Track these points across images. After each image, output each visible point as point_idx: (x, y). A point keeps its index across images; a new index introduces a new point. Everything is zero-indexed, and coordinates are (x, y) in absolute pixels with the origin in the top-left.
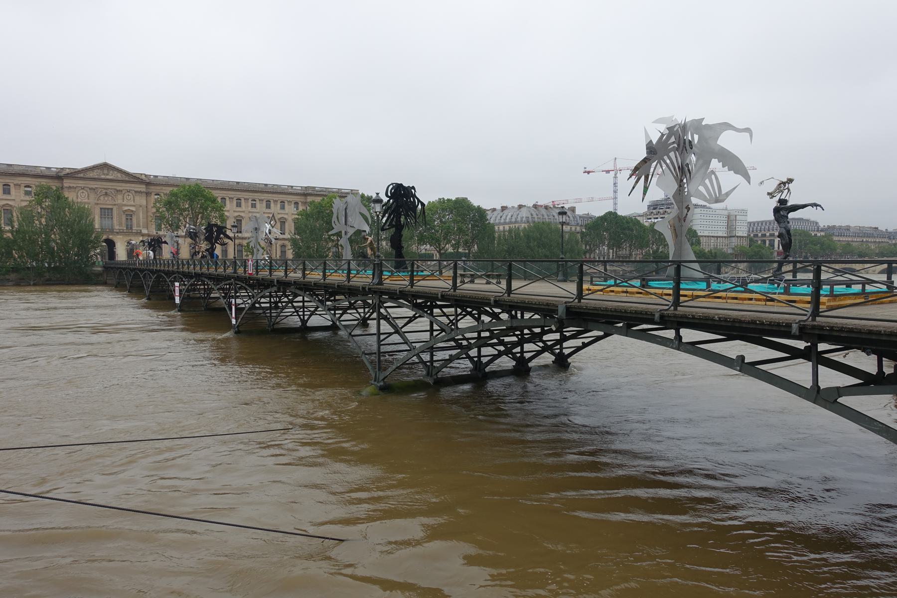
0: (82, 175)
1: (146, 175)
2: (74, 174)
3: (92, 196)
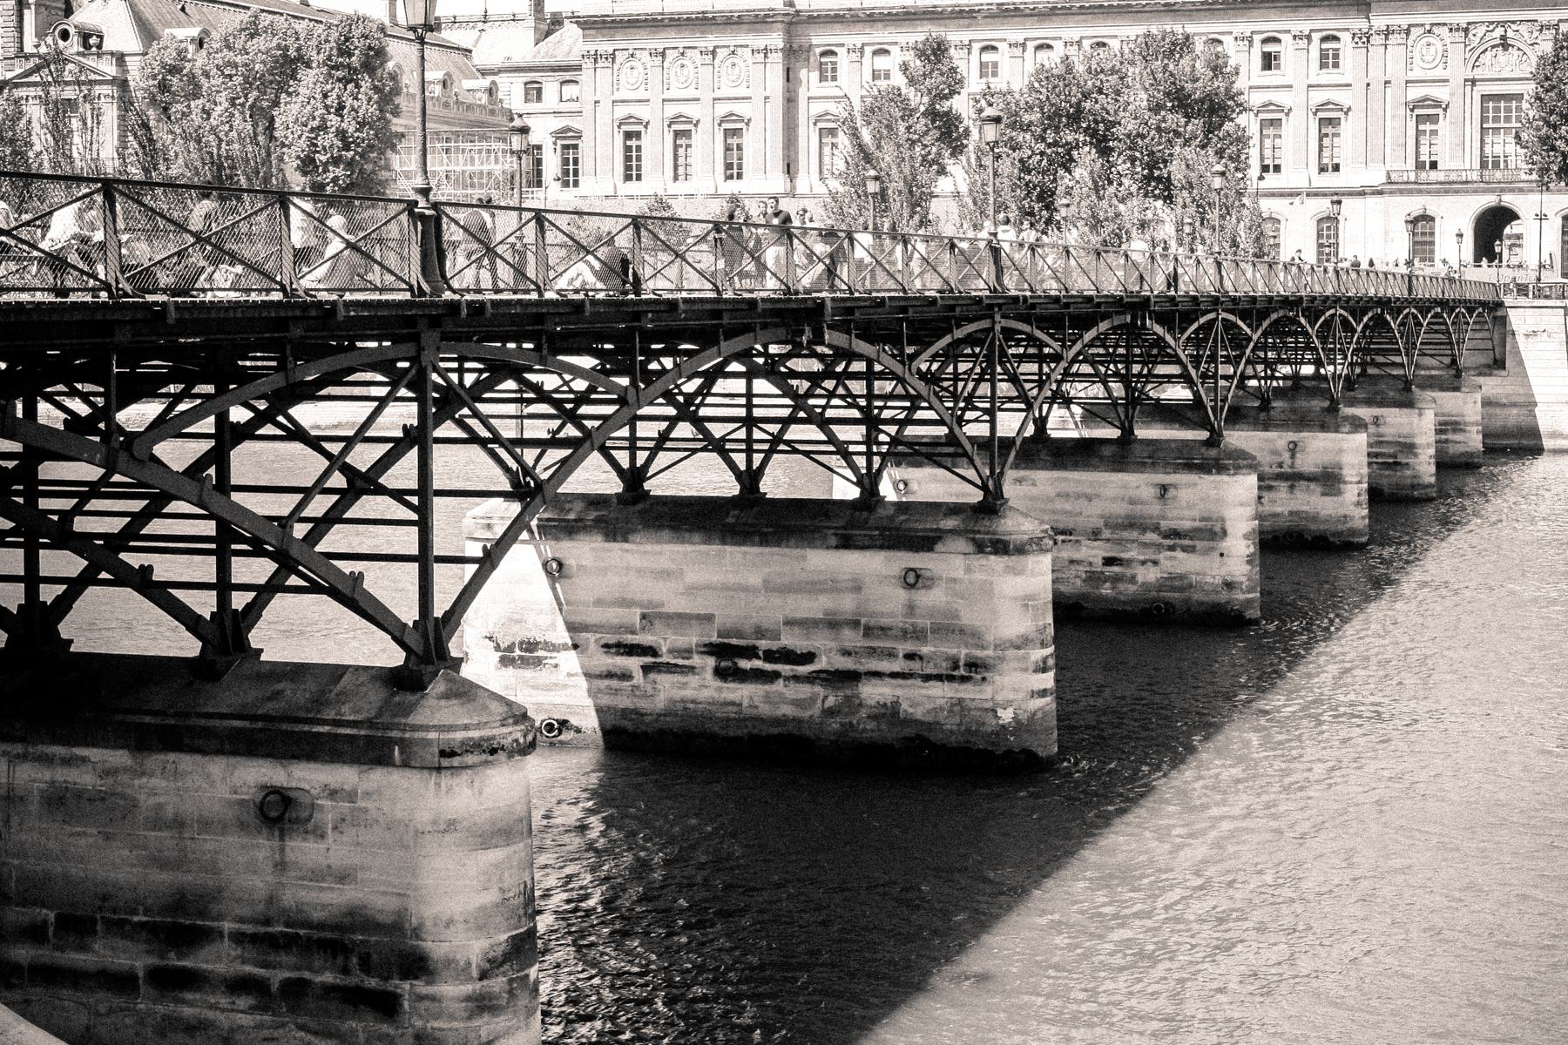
3: (1457, 54)
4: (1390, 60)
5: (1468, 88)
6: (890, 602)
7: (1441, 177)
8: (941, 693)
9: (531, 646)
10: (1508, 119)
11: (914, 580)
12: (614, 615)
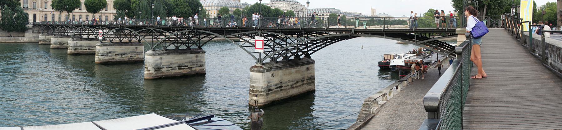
6: (194, 59)
8: (199, 68)
9: (158, 68)
11: (197, 57)
12: (167, 64)
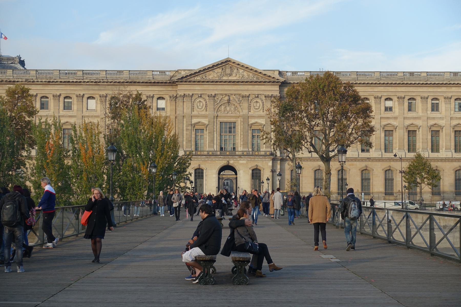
0: (198, 78)
1: (280, 73)
2: (189, 78)
4: (185, 108)
5: (215, 119)
7: (206, 153)
10: (230, 132)
